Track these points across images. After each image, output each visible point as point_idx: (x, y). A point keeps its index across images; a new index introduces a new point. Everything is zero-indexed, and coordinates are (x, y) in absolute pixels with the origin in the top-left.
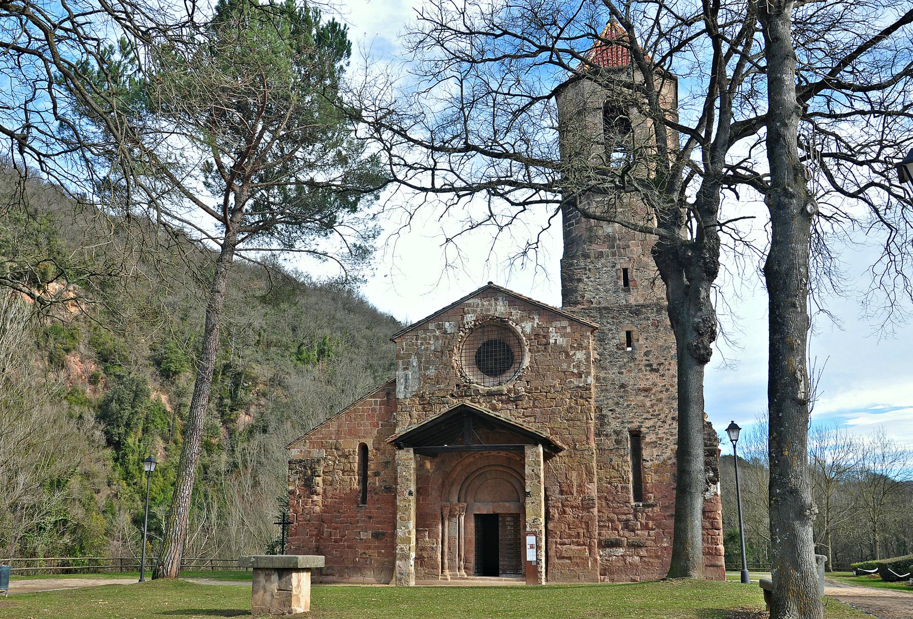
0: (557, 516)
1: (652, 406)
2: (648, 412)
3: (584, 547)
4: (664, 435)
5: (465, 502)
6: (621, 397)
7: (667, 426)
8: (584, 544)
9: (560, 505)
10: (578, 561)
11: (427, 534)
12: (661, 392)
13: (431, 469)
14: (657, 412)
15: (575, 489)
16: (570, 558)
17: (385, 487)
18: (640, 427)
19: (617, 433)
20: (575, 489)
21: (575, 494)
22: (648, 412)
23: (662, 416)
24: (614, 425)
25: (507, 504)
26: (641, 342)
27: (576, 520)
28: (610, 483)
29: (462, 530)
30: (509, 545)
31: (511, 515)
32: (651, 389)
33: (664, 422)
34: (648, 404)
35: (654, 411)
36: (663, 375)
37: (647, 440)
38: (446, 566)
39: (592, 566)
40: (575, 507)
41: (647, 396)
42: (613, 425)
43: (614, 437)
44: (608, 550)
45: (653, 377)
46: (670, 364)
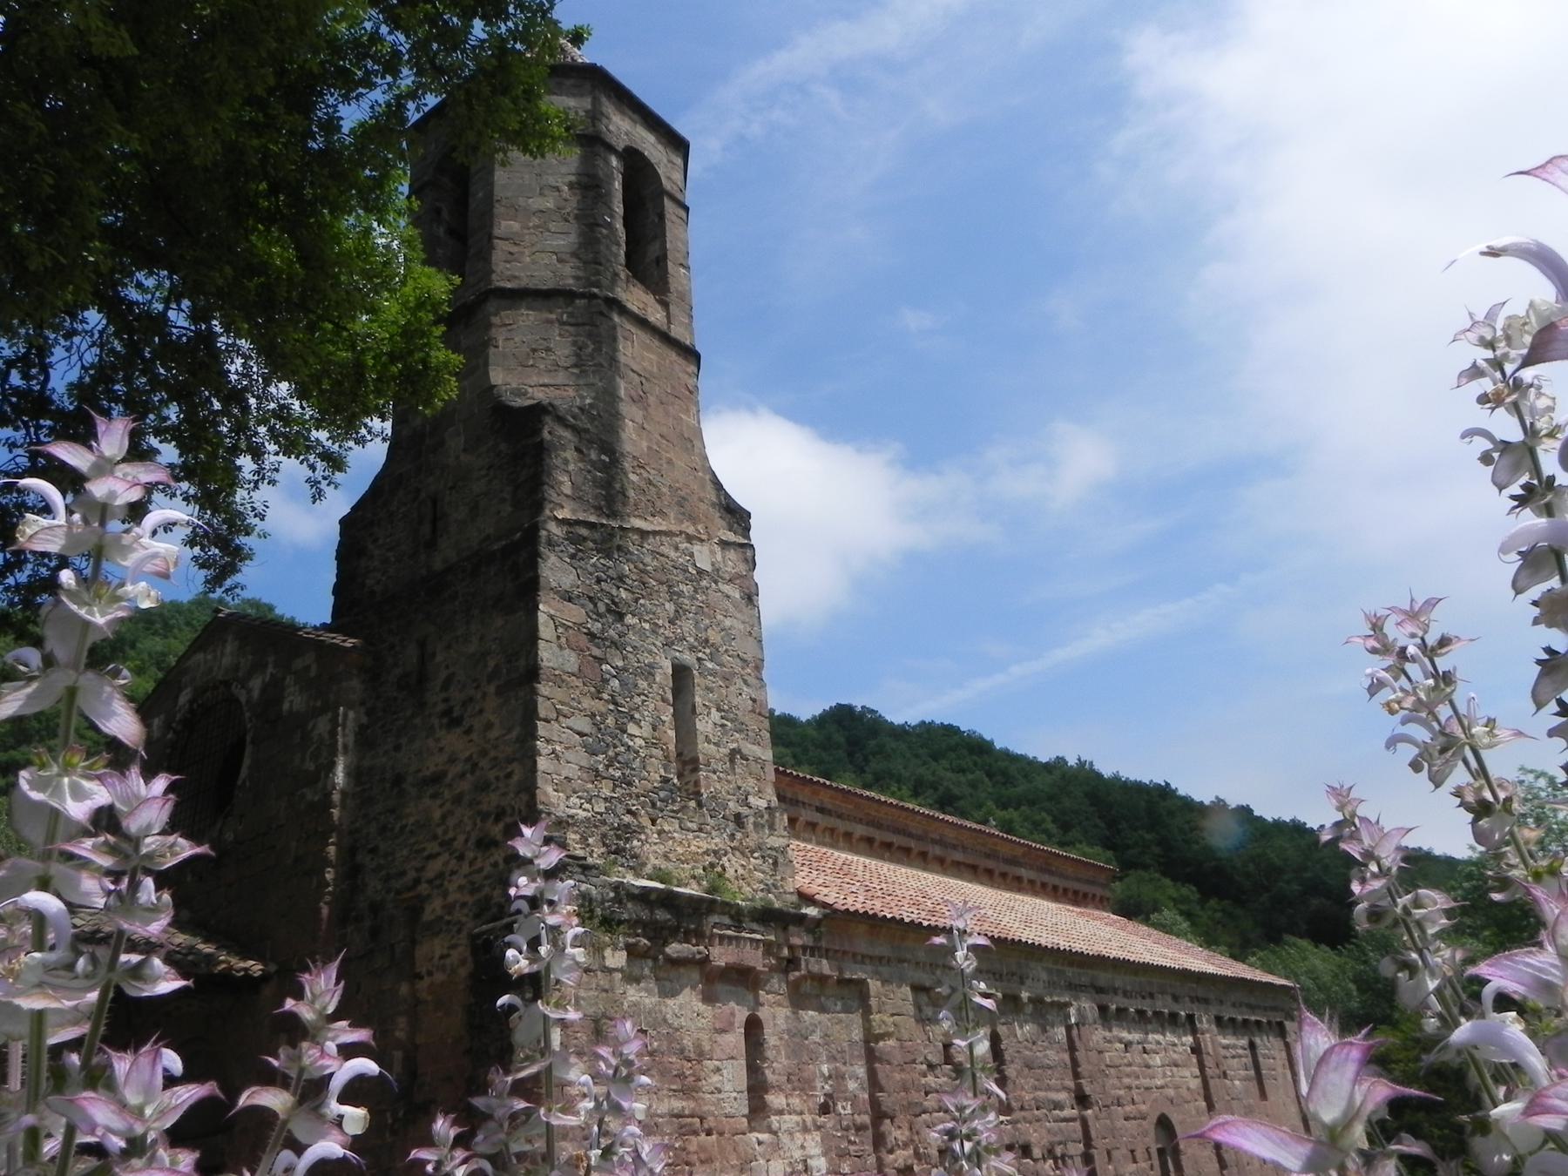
1: (444, 817)
2: (435, 837)
4: (458, 896)
6: (392, 811)
7: (465, 869)
12: (462, 776)
14: (451, 835)
18: (417, 882)
19: (375, 908)
22: (435, 837)
23: (458, 844)
24: (373, 885)
26: (439, 658)
32: (444, 774)
33: (461, 858)
34: (437, 814)
35: (445, 832)
36: (468, 731)
37: (427, 916)
41: (434, 796)
45: (453, 741)
46: (484, 695)
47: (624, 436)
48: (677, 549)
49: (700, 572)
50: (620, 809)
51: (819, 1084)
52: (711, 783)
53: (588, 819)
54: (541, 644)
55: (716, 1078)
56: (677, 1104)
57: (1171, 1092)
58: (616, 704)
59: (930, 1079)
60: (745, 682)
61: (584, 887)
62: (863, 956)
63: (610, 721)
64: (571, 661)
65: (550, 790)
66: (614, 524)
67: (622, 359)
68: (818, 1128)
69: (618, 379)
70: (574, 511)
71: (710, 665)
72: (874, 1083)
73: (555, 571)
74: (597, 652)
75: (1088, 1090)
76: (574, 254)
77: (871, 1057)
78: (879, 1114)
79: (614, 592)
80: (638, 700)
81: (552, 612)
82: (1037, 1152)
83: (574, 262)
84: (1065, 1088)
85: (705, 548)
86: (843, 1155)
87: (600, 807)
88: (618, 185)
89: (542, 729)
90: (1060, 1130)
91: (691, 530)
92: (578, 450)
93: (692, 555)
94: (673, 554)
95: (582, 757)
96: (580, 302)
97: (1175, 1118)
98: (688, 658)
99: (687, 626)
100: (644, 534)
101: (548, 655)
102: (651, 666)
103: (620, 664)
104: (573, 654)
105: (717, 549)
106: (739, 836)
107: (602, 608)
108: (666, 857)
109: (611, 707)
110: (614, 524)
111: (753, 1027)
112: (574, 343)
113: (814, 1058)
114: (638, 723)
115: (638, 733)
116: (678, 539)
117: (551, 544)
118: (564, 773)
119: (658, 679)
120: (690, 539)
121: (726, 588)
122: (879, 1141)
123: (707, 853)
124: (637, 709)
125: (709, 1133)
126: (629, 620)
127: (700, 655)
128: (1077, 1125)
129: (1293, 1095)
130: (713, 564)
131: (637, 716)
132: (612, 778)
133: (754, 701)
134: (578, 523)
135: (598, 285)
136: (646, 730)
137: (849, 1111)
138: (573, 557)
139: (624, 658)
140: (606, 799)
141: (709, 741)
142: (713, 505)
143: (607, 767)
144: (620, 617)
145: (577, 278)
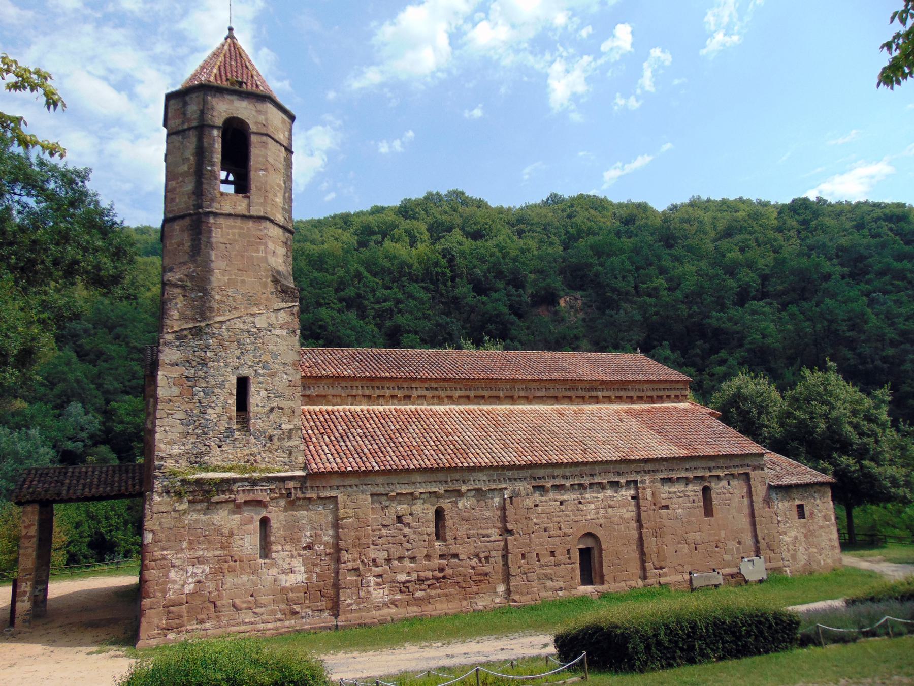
47: (213, 279)
48: (244, 322)
49: (259, 329)
50: (199, 446)
51: (303, 540)
52: (257, 424)
53: (180, 454)
54: (159, 389)
55: (240, 542)
56: (218, 553)
57: (602, 521)
58: (200, 403)
59: (384, 532)
60: (286, 374)
61: (165, 483)
62: (338, 487)
63: (196, 412)
64: (176, 391)
65: (162, 446)
66: (203, 324)
67: (214, 240)
68: (300, 555)
69: (211, 252)
70: (179, 326)
71: (261, 372)
72: (337, 537)
73: (169, 355)
74: (190, 384)
75: (510, 526)
76: (194, 193)
77: (336, 526)
78: (338, 550)
79: (203, 354)
80: (214, 398)
81: (165, 373)
82: (461, 557)
83: (194, 197)
84: (494, 527)
85: (264, 317)
86: (315, 565)
87: (190, 446)
88: (218, 146)
89: (158, 422)
90: (486, 546)
91: (256, 310)
92: (184, 296)
93: (254, 323)
94: (242, 326)
95: (181, 429)
96: (195, 218)
97: (599, 533)
98: (245, 372)
99: (248, 358)
100: (221, 322)
101: (162, 392)
102: (223, 381)
103: (204, 385)
104: (176, 388)
105: (273, 315)
106: (268, 445)
107: (194, 364)
108: (223, 460)
109: (198, 405)
110: (203, 324)
111: (265, 522)
112: (192, 240)
113: (301, 529)
114: (214, 408)
115: (212, 414)
116: (245, 318)
117: (165, 344)
118: (170, 437)
119: (227, 386)
120: (252, 315)
121: (278, 332)
122: (338, 561)
123: (247, 455)
124: (214, 402)
125: (235, 561)
126: (211, 364)
127: (255, 368)
128: (502, 543)
129: (746, 511)
130: (269, 323)
131: (213, 405)
132: (197, 434)
133: (291, 381)
134: (182, 330)
135: (201, 207)
136: (219, 409)
137: (322, 547)
138: (177, 346)
139: (207, 382)
140: (192, 443)
141: (257, 405)
142: (272, 293)
143: (194, 430)
144: (206, 364)
145: (194, 205)
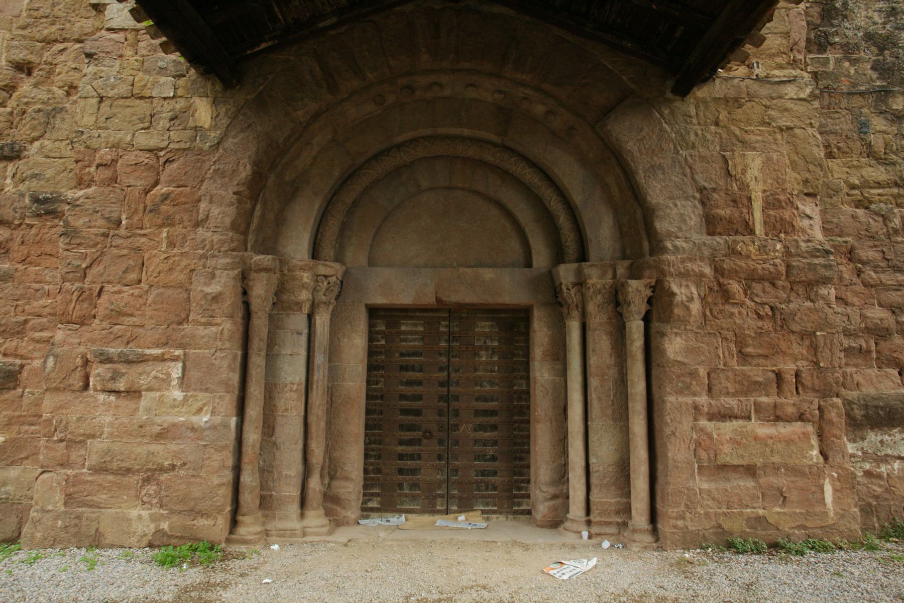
0: (696, 307)
3: (798, 426)
5: (339, 259)
8: (801, 418)
9: (708, 270)
10: (781, 481)
11: (176, 371)
13: (214, 127)
15: (758, 215)
16: (750, 471)
17: (36, 200)
20: (758, 215)
21: (759, 229)
25: (488, 274)
27: (767, 325)
28: (863, 204)
29: (320, 359)
30: (486, 413)
31: (491, 312)
38: (248, 498)
39: (836, 500)
40: (761, 279)
42: (861, 21)
43: (868, 55)
44: (873, 437)
